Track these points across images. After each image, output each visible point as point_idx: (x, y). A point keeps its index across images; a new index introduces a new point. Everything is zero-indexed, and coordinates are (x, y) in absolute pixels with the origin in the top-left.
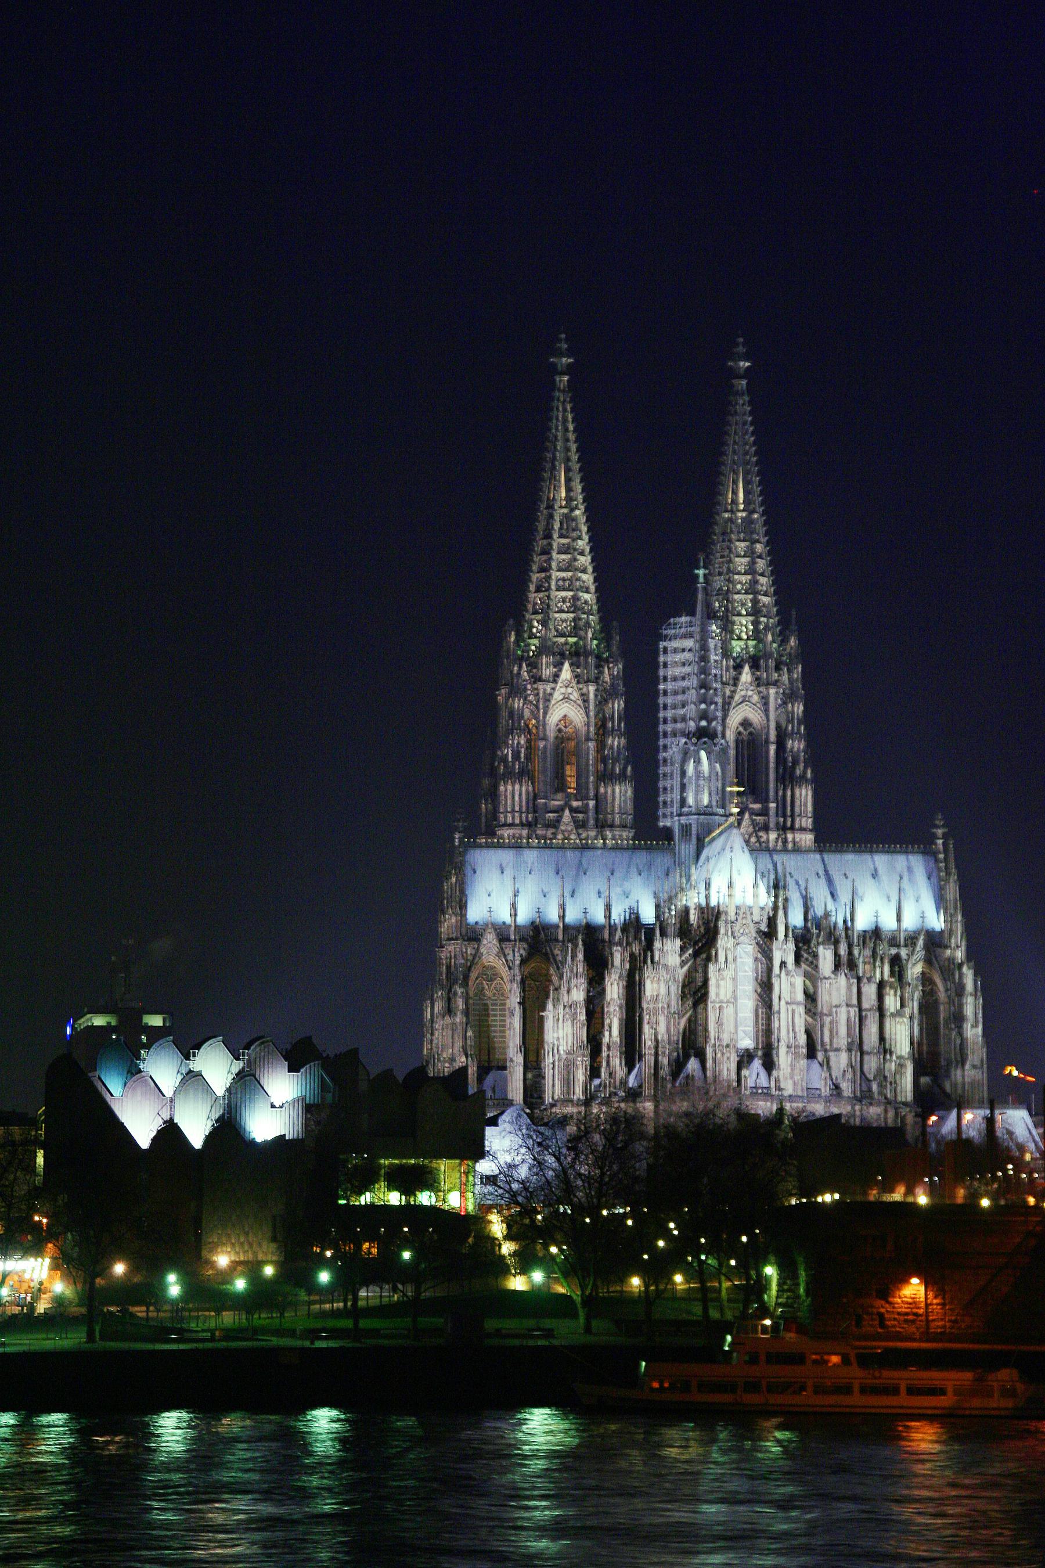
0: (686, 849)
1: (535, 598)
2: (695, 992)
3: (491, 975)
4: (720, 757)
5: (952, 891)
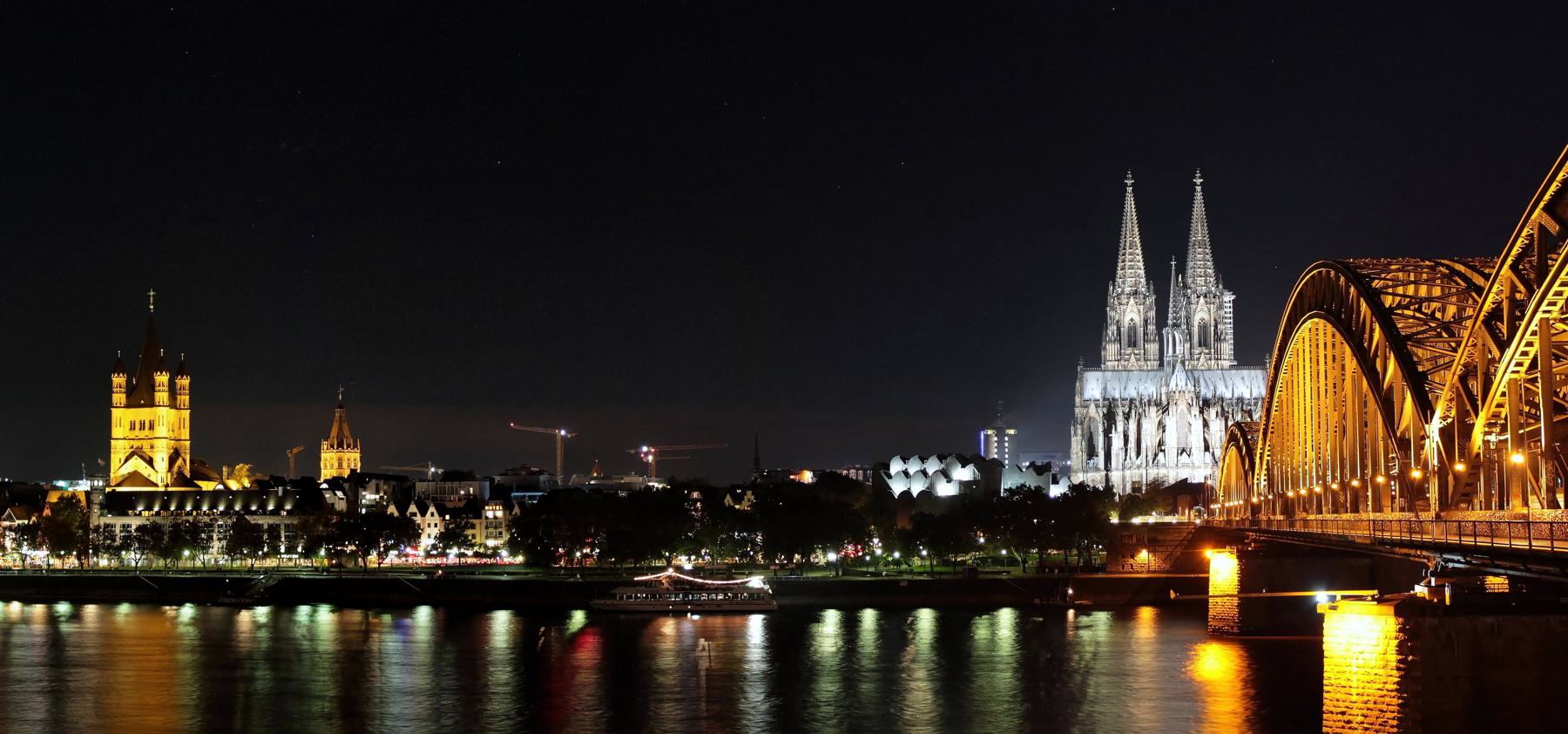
0: (1168, 369)
1: (1120, 272)
2: (1161, 426)
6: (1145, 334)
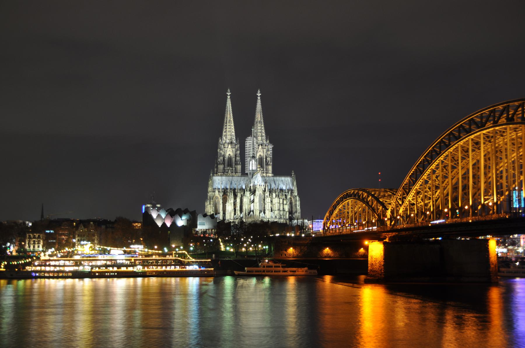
0: (250, 176)
1: (224, 134)
3: (217, 198)
4: (256, 161)
5: (295, 183)
6: (235, 161)
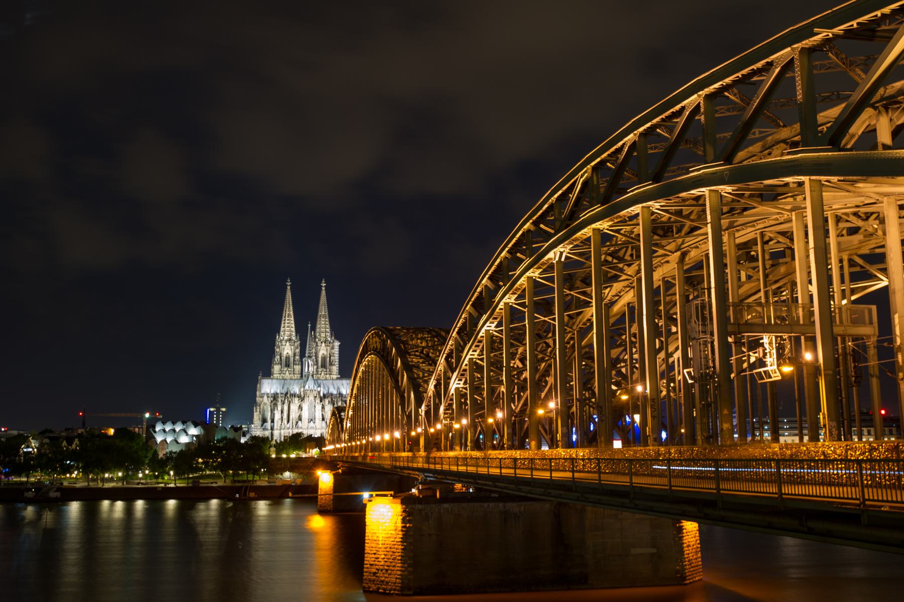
0: (305, 379)
2: (300, 408)
3: (265, 404)
